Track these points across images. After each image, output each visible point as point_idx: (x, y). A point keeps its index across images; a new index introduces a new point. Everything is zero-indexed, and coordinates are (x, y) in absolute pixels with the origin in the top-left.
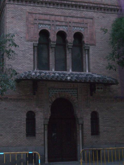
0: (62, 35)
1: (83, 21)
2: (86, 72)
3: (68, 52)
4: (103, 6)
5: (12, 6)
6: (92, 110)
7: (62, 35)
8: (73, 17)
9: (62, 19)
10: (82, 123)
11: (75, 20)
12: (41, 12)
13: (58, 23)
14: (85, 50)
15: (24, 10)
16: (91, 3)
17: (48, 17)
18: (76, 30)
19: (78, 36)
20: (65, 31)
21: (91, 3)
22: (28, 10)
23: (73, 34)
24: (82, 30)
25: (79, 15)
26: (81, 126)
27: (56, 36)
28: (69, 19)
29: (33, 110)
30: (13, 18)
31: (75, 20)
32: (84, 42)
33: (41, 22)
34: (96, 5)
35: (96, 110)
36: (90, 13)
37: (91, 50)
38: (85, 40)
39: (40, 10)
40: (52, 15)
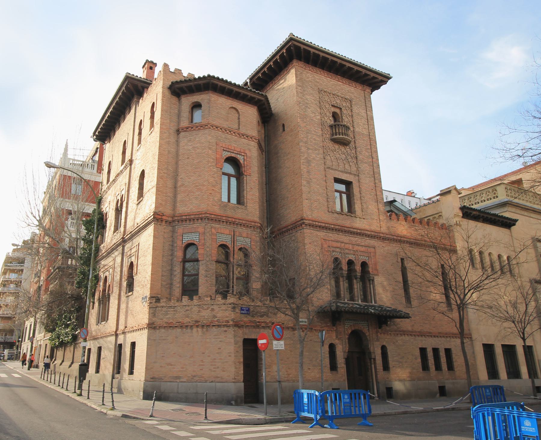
0: (350, 263)
1: (367, 250)
2: (372, 303)
3: (355, 281)
4: (382, 235)
5: (308, 231)
6: (382, 344)
7: (350, 263)
8: (358, 245)
9: (351, 246)
10: (374, 357)
11: (360, 248)
12: (332, 239)
13: (347, 251)
14: (369, 280)
15: (319, 236)
16: (373, 232)
17: (338, 245)
18: (363, 258)
19: (364, 265)
20: (353, 259)
21: (373, 232)
22: (322, 237)
23: (360, 263)
24: (367, 259)
25: (363, 244)
26: (373, 360)
27: (346, 265)
28: (356, 248)
29: (333, 342)
30: (310, 243)
31: (360, 248)
32: (369, 271)
33: (334, 249)
34: (376, 234)
35: (384, 344)
36: (372, 242)
37: (375, 280)
38: (370, 270)
39: (331, 237)
40: (342, 243)
